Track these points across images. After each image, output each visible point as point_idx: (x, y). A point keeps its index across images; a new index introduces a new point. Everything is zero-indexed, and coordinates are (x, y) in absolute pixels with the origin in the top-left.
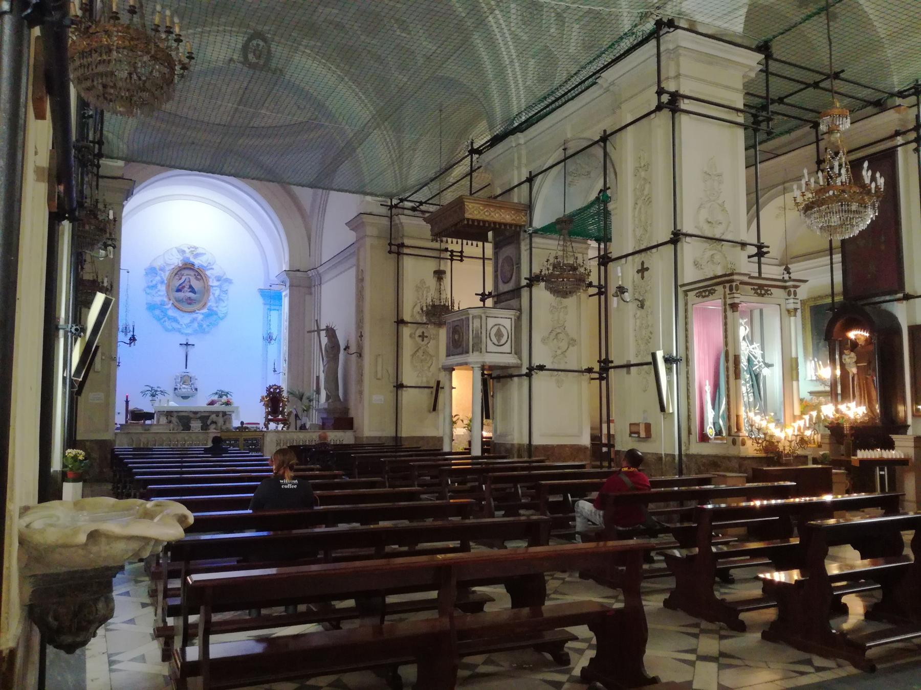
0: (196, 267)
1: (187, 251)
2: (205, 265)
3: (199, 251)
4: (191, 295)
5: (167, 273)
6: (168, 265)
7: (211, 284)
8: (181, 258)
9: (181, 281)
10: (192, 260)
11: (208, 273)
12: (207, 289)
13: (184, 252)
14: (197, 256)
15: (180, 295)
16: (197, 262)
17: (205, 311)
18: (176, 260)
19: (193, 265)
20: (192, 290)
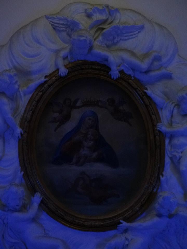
0: (115, 73)
1: (84, 23)
2: (144, 65)
3: (124, 19)
4: (100, 169)
5: (24, 101)
6: (24, 73)
7: (164, 127)
8: (66, 49)
9: (69, 127)
10: (100, 50)
11: (156, 92)
12: (151, 150)
13: (72, 26)
14: (116, 35)
15: (71, 171)
16: (116, 58)
17: (149, 221)
18: (46, 56)
19: (104, 66)
20: (106, 154)
